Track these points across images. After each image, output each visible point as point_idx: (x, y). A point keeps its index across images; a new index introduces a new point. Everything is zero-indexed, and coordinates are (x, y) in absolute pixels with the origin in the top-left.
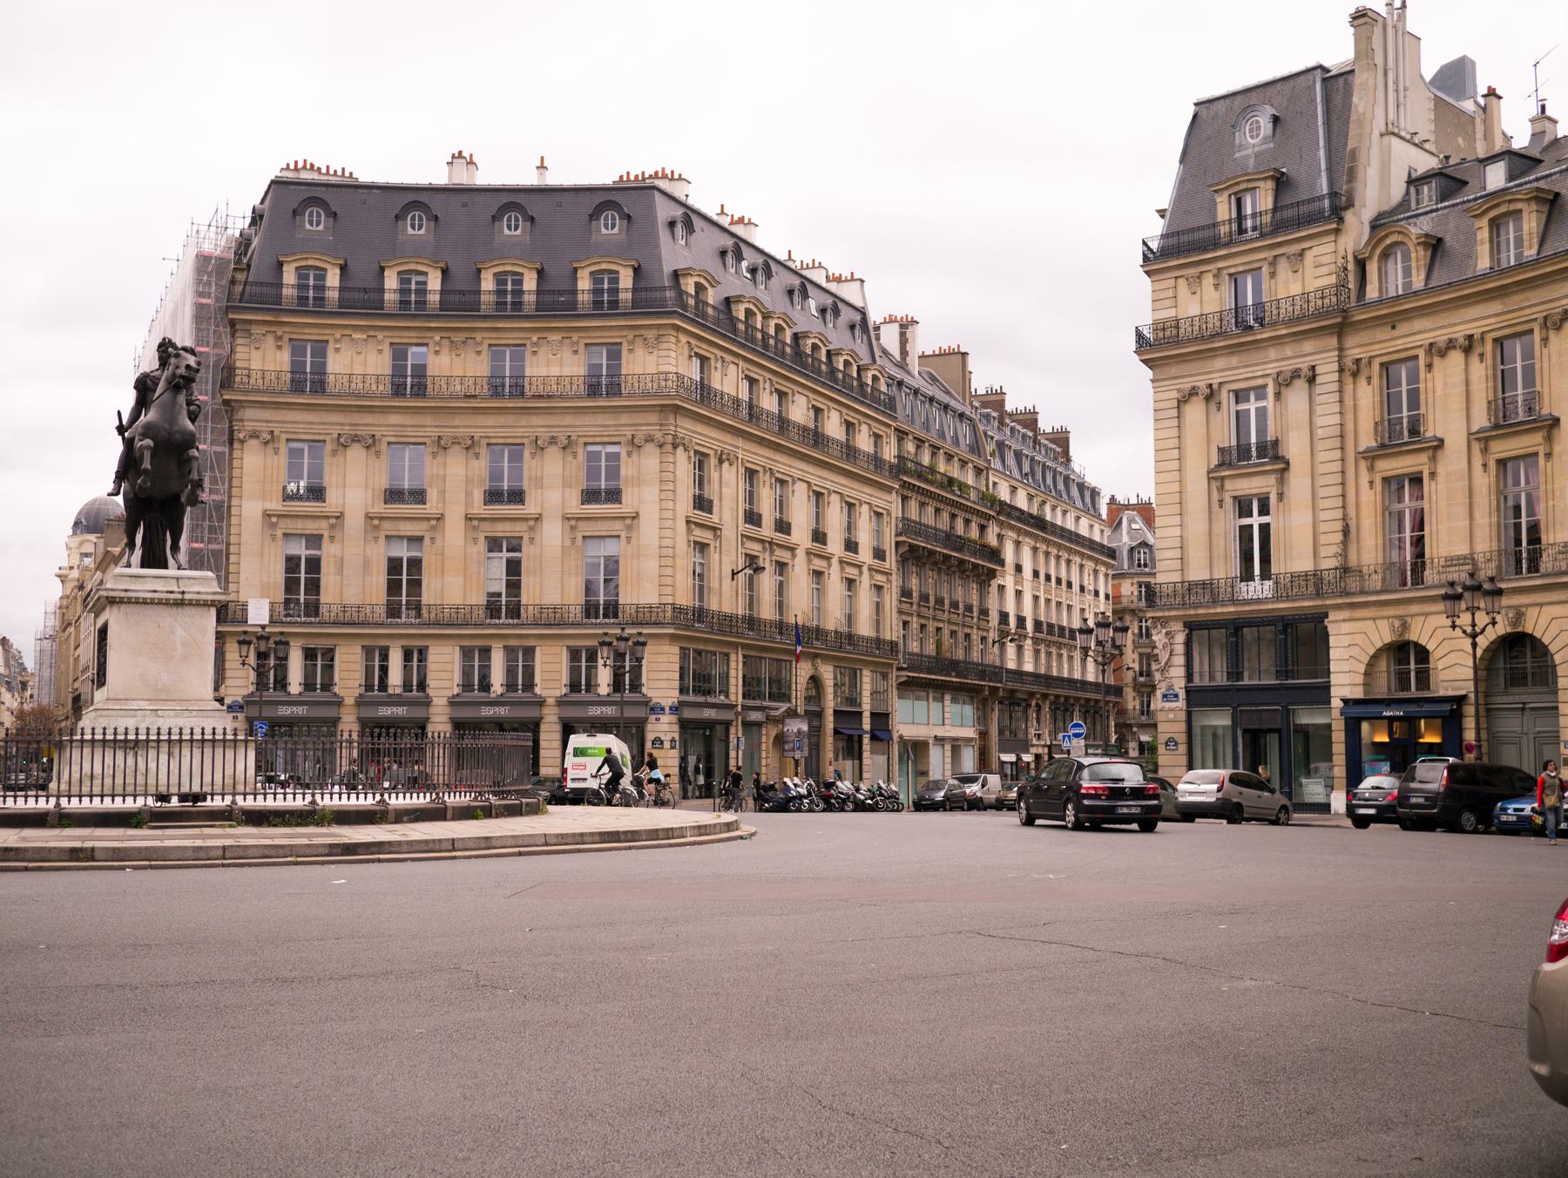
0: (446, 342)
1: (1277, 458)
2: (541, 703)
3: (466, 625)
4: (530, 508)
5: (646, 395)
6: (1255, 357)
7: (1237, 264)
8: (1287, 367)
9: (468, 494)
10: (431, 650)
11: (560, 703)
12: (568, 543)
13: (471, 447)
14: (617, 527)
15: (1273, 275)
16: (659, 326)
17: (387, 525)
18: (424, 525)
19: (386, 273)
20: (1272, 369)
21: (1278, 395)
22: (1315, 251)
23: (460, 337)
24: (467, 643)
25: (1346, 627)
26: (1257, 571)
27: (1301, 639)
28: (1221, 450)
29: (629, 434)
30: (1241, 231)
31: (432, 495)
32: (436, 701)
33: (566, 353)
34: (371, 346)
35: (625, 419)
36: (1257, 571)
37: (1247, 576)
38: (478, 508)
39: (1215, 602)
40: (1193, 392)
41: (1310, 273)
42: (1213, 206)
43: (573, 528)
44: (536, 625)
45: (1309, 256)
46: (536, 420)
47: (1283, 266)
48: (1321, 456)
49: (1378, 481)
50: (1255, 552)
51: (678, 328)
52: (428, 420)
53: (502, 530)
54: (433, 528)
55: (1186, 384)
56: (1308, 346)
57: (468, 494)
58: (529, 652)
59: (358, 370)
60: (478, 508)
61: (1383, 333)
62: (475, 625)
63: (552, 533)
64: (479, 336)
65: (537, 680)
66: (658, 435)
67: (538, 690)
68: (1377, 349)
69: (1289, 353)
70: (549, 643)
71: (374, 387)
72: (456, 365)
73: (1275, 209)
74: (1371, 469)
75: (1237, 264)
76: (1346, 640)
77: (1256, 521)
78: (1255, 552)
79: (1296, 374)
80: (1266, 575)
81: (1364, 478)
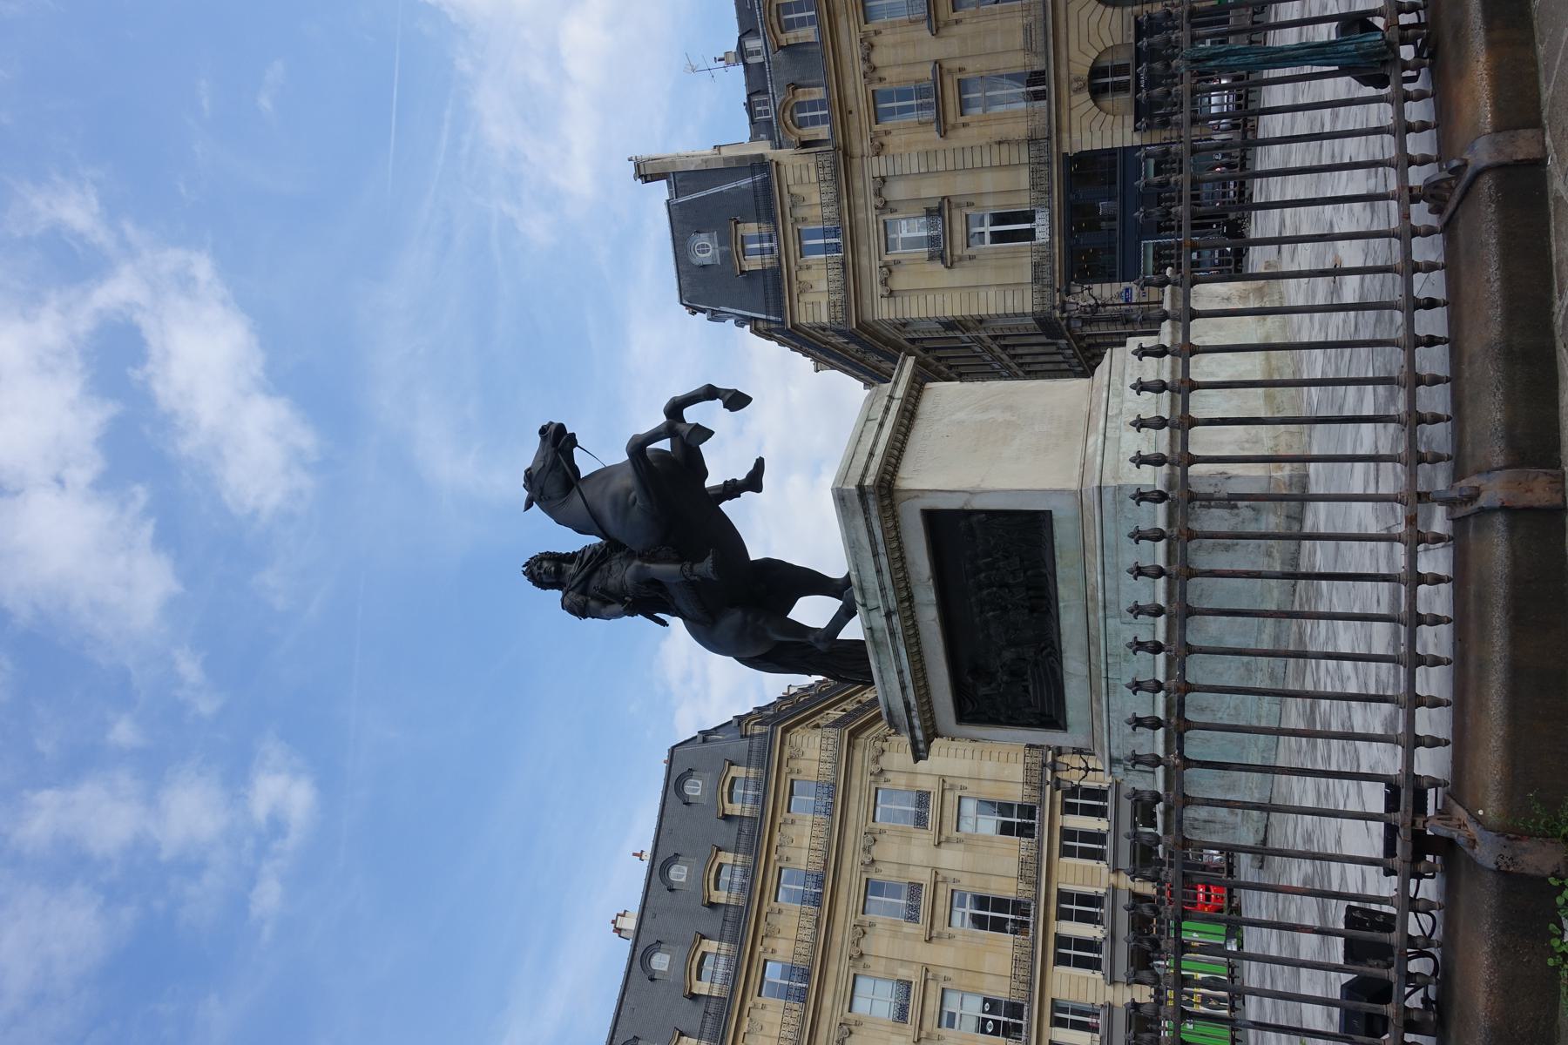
0: (766, 941)
1: (940, 210)
2: (1114, 889)
3: (1033, 959)
4: (925, 877)
5: (837, 763)
6: (862, 230)
7: (793, 248)
8: (873, 201)
9: (907, 936)
10: (1056, 996)
11: (1116, 870)
12: (961, 846)
13: (862, 931)
14: (951, 797)
15: (804, 220)
16: (782, 743)
17: (927, 1025)
18: (931, 984)
19: (695, 991)
20: (872, 214)
21: (893, 211)
22: (791, 182)
23: (763, 925)
24: (1051, 957)
25: (1076, 136)
26: (1027, 226)
27: (1086, 176)
28: (931, 258)
29: (870, 778)
30: (772, 249)
31: (903, 973)
32: (1109, 998)
33: (791, 831)
34: (755, 1014)
35: (855, 782)
36: (1027, 226)
37: (1030, 235)
38: (919, 929)
39: (1051, 257)
40: (885, 282)
41: (802, 176)
42: (750, 275)
43: (948, 840)
44: (1037, 884)
45: (794, 190)
46: (847, 864)
47: (800, 212)
48: (941, 167)
49: (962, 120)
50: (1011, 226)
51: (786, 730)
52: (833, 968)
53: (942, 909)
54: (935, 978)
55: (879, 290)
56: (858, 184)
57: (907, 936)
58: (1064, 896)
59: (776, 1032)
60: (919, 929)
61: (854, 121)
62: (1034, 946)
63: (950, 858)
64: (765, 909)
65: (1090, 890)
66: (873, 753)
67: (1102, 891)
68: (865, 126)
69: (862, 201)
70: (1054, 873)
71: (795, 1014)
72: (787, 936)
73: (758, 221)
74: (954, 127)
75: (793, 248)
76: (1087, 135)
77: (988, 229)
78: (1011, 226)
79: (878, 193)
80: (1029, 217)
81: (962, 132)
